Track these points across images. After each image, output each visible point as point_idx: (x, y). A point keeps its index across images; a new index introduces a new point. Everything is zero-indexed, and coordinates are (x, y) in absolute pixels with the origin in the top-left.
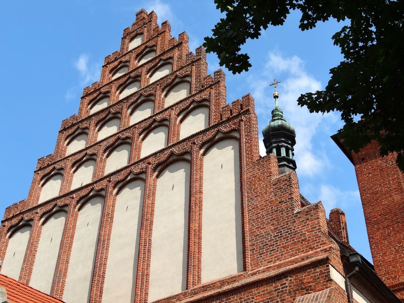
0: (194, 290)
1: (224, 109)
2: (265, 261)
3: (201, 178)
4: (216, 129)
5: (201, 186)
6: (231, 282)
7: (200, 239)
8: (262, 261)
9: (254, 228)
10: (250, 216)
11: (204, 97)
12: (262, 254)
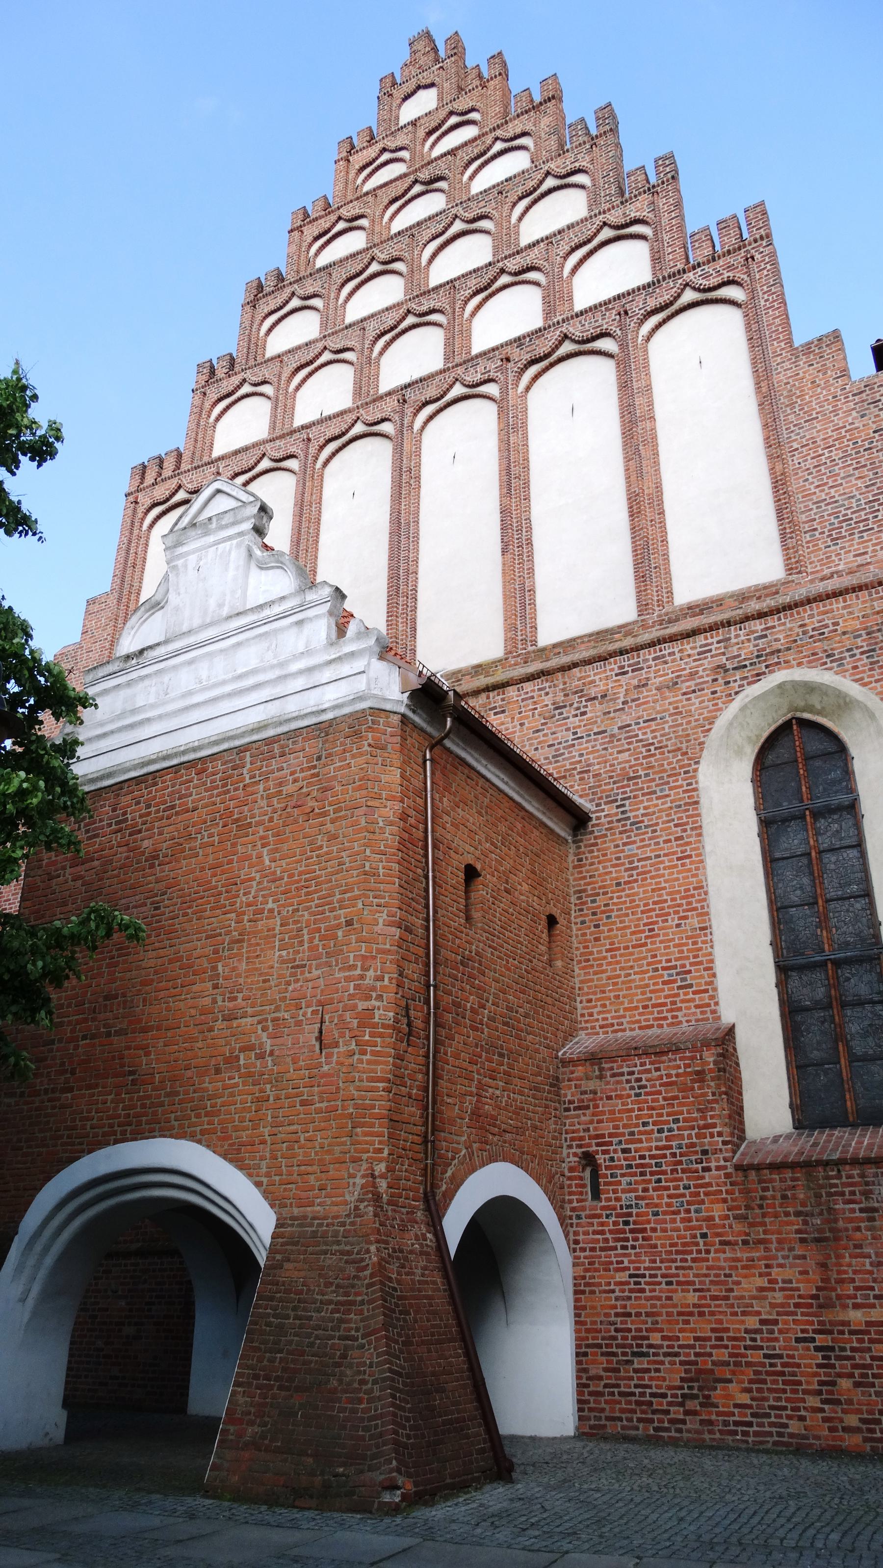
0: (667, 614)
1: (696, 237)
2: (846, 553)
3: (649, 388)
4: (680, 281)
5: (651, 404)
6: (767, 596)
7: (662, 513)
8: (839, 554)
9: (812, 487)
10: (796, 462)
11: (633, 215)
12: (837, 539)
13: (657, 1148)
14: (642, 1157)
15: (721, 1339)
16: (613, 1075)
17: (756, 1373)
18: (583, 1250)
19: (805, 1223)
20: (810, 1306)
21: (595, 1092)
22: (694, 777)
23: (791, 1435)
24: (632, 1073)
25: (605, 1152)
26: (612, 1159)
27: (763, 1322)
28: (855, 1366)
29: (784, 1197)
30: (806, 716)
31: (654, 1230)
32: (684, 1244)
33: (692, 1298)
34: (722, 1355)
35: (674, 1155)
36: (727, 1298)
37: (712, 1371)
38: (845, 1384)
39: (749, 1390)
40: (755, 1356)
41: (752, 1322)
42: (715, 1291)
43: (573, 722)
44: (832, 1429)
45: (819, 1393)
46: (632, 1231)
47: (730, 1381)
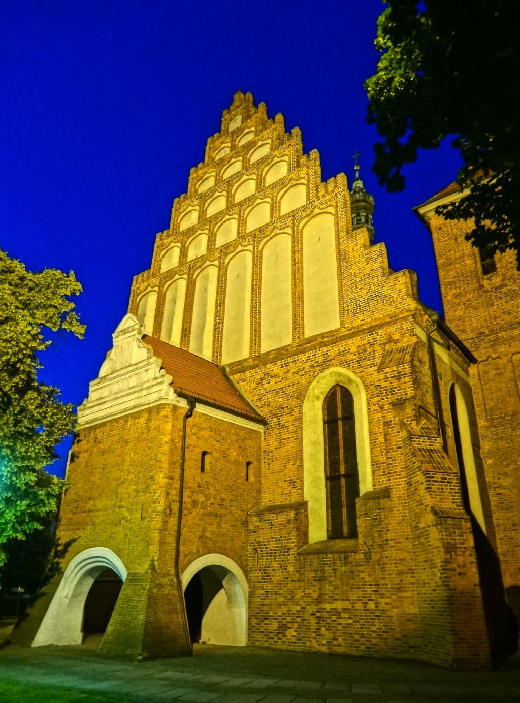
13: (276, 547)
14: (271, 550)
15: (289, 614)
16: (264, 521)
17: (299, 625)
18: (252, 582)
19: (316, 574)
20: (315, 602)
21: (258, 527)
22: (302, 408)
23: (307, 647)
24: (269, 520)
25: (260, 548)
26: (262, 551)
27: (302, 608)
28: (327, 623)
29: (311, 565)
30: (341, 384)
31: (273, 576)
32: (281, 581)
33: (282, 599)
34: (289, 619)
35: (280, 549)
36: (292, 600)
37: (286, 625)
38: (323, 629)
39: (295, 631)
40: (299, 620)
41: (299, 608)
42: (289, 597)
43: (266, 386)
44: (319, 645)
45: (315, 632)
46: (267, 576)
47: (291, 628)
